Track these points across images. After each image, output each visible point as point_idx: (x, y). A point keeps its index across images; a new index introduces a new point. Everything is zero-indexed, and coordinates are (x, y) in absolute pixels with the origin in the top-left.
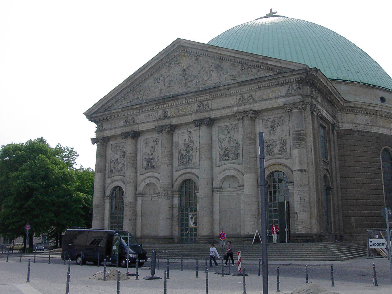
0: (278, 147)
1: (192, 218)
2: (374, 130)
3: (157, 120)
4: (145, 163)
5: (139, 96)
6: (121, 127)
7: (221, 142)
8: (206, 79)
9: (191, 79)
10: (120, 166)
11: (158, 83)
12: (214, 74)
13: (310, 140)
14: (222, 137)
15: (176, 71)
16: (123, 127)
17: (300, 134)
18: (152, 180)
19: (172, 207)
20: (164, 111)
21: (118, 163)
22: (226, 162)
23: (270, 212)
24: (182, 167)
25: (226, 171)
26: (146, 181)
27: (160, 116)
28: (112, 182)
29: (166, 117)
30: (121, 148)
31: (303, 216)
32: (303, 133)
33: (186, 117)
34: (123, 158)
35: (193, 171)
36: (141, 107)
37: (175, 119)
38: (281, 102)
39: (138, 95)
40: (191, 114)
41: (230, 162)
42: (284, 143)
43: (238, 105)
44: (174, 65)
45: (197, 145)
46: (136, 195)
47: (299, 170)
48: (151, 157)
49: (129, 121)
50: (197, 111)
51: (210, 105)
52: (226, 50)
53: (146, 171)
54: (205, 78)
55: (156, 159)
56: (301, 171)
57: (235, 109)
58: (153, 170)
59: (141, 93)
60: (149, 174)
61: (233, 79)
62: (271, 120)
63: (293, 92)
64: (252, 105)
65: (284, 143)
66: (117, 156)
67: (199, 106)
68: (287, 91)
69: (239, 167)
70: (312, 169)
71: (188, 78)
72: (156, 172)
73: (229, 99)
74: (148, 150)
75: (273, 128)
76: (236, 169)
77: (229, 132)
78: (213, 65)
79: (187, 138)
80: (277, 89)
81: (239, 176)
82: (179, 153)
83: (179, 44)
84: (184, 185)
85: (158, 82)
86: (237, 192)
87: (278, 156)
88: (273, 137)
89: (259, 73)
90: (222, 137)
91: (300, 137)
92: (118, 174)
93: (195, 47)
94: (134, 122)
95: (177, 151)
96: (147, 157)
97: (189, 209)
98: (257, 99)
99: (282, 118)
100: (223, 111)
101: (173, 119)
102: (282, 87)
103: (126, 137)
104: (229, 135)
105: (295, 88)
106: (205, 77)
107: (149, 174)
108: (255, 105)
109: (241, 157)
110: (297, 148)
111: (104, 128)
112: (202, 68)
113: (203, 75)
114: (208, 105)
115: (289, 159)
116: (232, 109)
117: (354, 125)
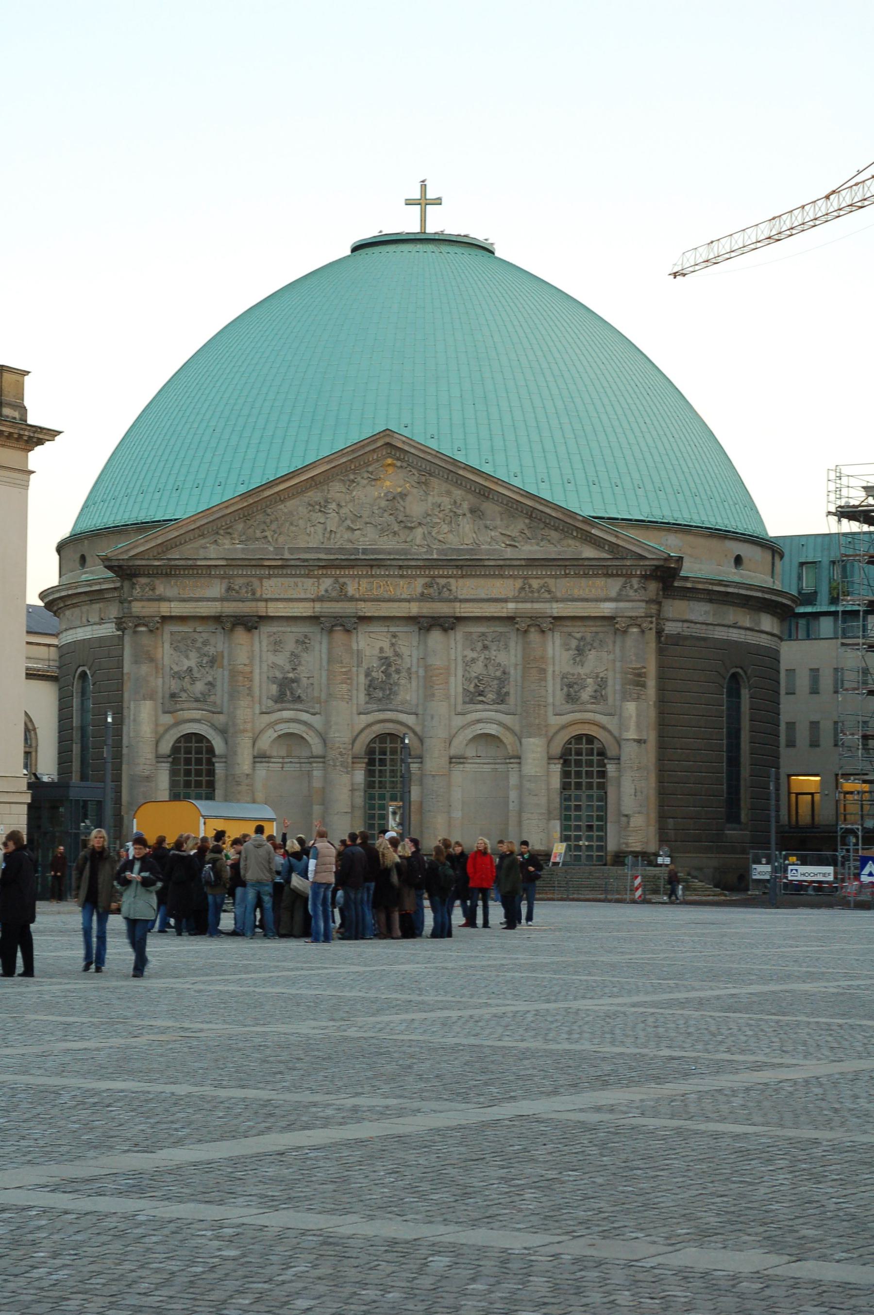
0: (589, 690)
1: (394, 813)
3: (320, 599)
4: (274, 689)
5: (267, 533)
6: (214, 600)
7: (469, 663)
8: (446, 531)
9: (413, 525)
10: (199, 687)
11: (319, 514)
12: (467, 526)
13: (651, 683)
14: (471, 655)
15: (369, 494)
17: (639, 675)
18: (295, 728)
20: (336, 582)
21: (193, 680)
22: (480, 707)
23: (568, 808)
24: (374, 707)
25: (481, 725)
26: (277, 727)
27: (326, 591)
28: (177, 724)
29: (344, 597)
30: (199, 645)
31: (637, 821)
32: (645, 673)
33: (396, 605)
34: (207, 669)
35: (403, 717)
36: (283, 567)
37: (369, 604)
38: (607, 608)
39: (263, 531)
40: (408, 601)
41: (487, 707)
42: (602, 683)
43: (516, 600)
44: (365, 482)
45: (407, 662)
47: (635, 740)
48: (291, 675)
49: (237, 587)
50: (422, 594)
51: (453, 588)
52: (504, 484)
53: (279, 706)
54: (445, 528)
55: (305, 681)
56: (639, 741)
58: (300, 706)
59: (274, 526)
60: (286, 714)
61: (510, 545)
62: (578, 636)
63: (631, 593)
64: (547, 605)
65: (602, 683)
66: (187, 663)
67: (427, 586)
68: (621, 590)
69: (507, 719)
70: (652, 737)
71: (404, 519)
72: (307, 712)
73: (498, 582)
74: (281, 659)
75: (580, 651)
76: (500, 724)
77: (485, 647)
78: (465, 505)
79: (386, 645)
80: (600, 582)
81: (508, 739)
82: (367, 675)
83: (387, 440)
85: (320, 511)
86: (492, 766)
87: (590, 707)
88: (579, 670)
89: (565, 542)
90: (471, 655)
91: (638, 679)
92: (195, 705)
93: (429, 458)
94: (254, 594)
95: (362, 671)
97: (388, 795)
98: (559, 595)
99: (601, 636)
100: (485, 605)
101: (361, 605)
102: (610, 580)
103: (234, 626)
104: (487, 652)
105: (636, 586)
106: (445, 526)
108: (555, 605)
109: (512, 700)
110: (634, 700)
111: (157, 592)
112: (440, 506)
113: (438, 521)
114: (447, 586)
115: (611, 715)
116: (504, 605)
117: (686, 625)
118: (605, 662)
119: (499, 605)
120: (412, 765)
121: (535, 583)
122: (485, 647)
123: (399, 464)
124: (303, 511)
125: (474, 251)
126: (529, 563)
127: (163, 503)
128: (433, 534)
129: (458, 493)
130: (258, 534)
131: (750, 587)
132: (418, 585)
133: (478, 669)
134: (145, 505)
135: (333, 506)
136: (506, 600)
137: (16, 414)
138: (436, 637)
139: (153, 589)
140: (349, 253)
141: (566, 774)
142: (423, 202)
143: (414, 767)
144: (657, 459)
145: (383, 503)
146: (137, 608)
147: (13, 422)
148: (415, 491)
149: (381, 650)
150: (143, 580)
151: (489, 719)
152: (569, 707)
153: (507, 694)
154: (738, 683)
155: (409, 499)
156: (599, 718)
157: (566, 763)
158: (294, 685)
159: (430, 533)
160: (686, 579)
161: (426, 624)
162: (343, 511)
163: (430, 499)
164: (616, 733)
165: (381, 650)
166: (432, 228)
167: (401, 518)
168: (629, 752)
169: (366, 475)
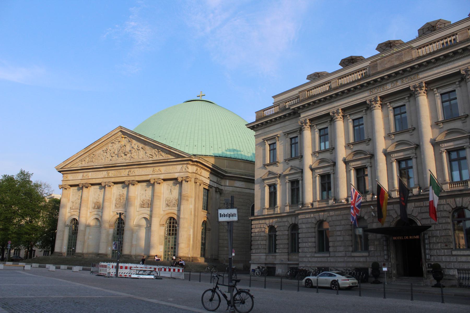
4: (94, 205)
19: (108, 235)
38: (176, 176)
63: (184, 170)
96: (95, 201)
119: (148, 176)
121: (157, 168)
124: (102, 152)
128: (132, 155)
129: (139, 144)
133: (144, 197)
152: (168, 208)
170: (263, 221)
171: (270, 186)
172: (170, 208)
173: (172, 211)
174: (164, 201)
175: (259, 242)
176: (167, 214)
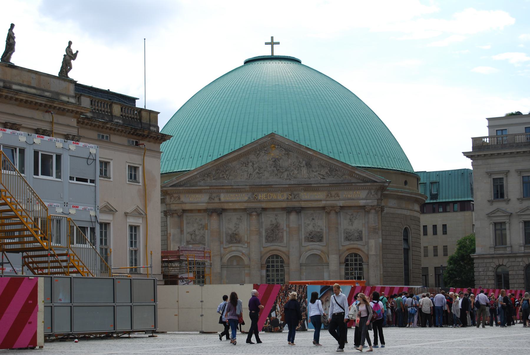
2: (399, 211)
5: (225, 176)
12: (304, 171)
15: (266, 159)
16: (208, 203)
24: (269, 244)
33: (277, 203)
38: (362, 203)
44: (263, 154)
46: (222, 267)
50: (288, 199)
54: (296, 172)
57: (323, 202)
59: (227, 173)
78: (304, 162)
82: (266, 232)
84: (271, 260)
89: (344, 177)
94: (220, 199)
96: (230, 232)
103: (212, 212)
105: (373, 193)
107: (234, 248)
111: (181, 200)
118: (359, 224)
120: (475, 261)
121: (333, 193)
122: (313, 219)
123: (277, 147)
125: (295, 63)
126: (331, 185)
127: (177, 164)
130: (221, 176)
131: (411, 193)
132: (285, 196)
133: (310, 228)
134: (170, 166)
135: (251, 164)
136: (321, 201)
137: (155, 129)
138: (293, 217)
139: (179, 198)
140: (243, 64)
141: (347, 269)
142: (272, 43)
143: (286, 268)
144: (373, 143)
145: (271, 162)
146: (173, 207)
147: (154, 132)
148: (283, 157)
149: (271, 221)
150: (175, 195)
151: (316, 247)
152: (348, 243)
153: (322, 237)
154: (407, 232)
155: (281, 161)
156: (359, 247)
157: (347, 265)
158: (237, 236)
159: (290, 174)
160: (388, 190)
161: (289, 211)
162: (255, 166)
163: (290, 160)
164: (366, 252)
165: (271, 221)
166: (276, 54)
167: (278, 168)
168: (372, 260)
169: (264, 151)
170: (491, 260)
171: (495, 224)
172: (352, 242)
173: (355, 246)
174: (343, 234)
175: (485, 281)
176: (348, 250)
